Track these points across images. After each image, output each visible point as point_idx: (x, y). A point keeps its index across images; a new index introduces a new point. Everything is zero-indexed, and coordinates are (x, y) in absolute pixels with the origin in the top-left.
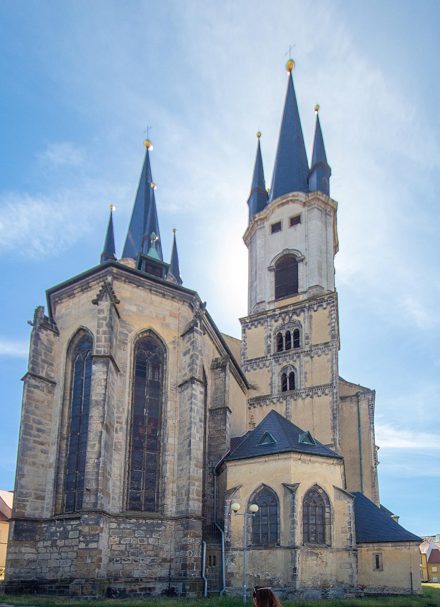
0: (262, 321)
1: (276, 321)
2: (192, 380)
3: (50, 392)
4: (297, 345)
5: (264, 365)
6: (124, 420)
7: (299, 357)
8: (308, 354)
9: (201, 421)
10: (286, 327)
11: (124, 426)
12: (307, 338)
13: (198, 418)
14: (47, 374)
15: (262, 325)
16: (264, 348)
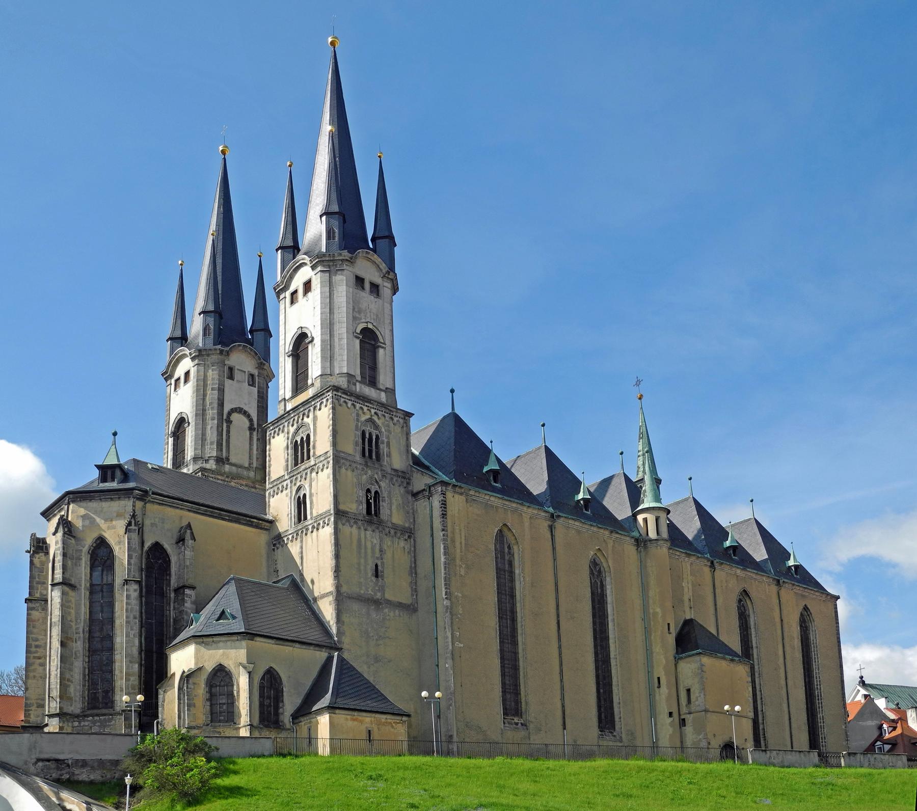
0: (281, 427)
1: (293, 425)
2: (126, 582)
3: (43, 609)
4: (309, 458)
5: (283, 487)
6: (81, 630)
7: (306, 474)
8: (312, 469)
9: (135, 618)
10: (300, 431)
11: (82, 635)
12: (314, 447)
13: (132, 616)
14: (41, 594)
15: (283, 432)
16: (284, 464)
